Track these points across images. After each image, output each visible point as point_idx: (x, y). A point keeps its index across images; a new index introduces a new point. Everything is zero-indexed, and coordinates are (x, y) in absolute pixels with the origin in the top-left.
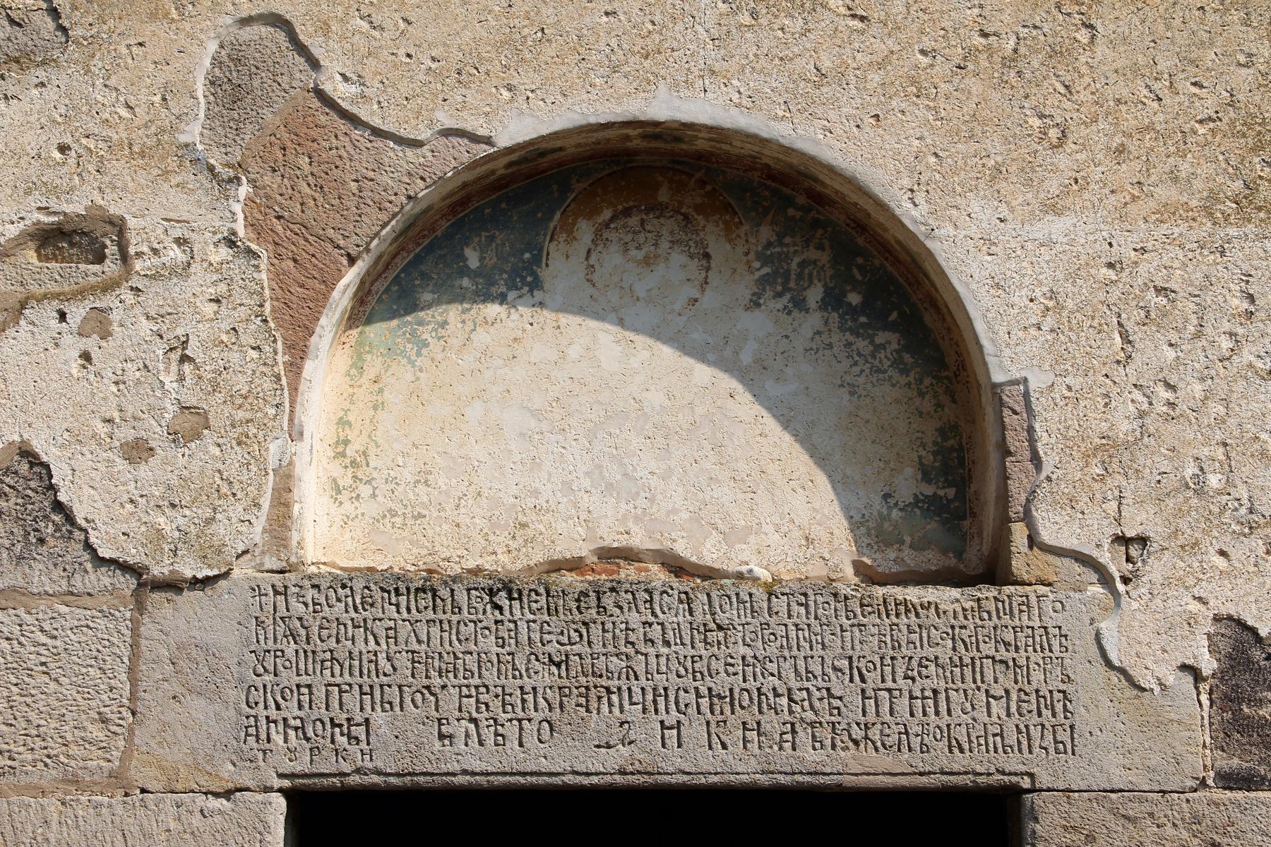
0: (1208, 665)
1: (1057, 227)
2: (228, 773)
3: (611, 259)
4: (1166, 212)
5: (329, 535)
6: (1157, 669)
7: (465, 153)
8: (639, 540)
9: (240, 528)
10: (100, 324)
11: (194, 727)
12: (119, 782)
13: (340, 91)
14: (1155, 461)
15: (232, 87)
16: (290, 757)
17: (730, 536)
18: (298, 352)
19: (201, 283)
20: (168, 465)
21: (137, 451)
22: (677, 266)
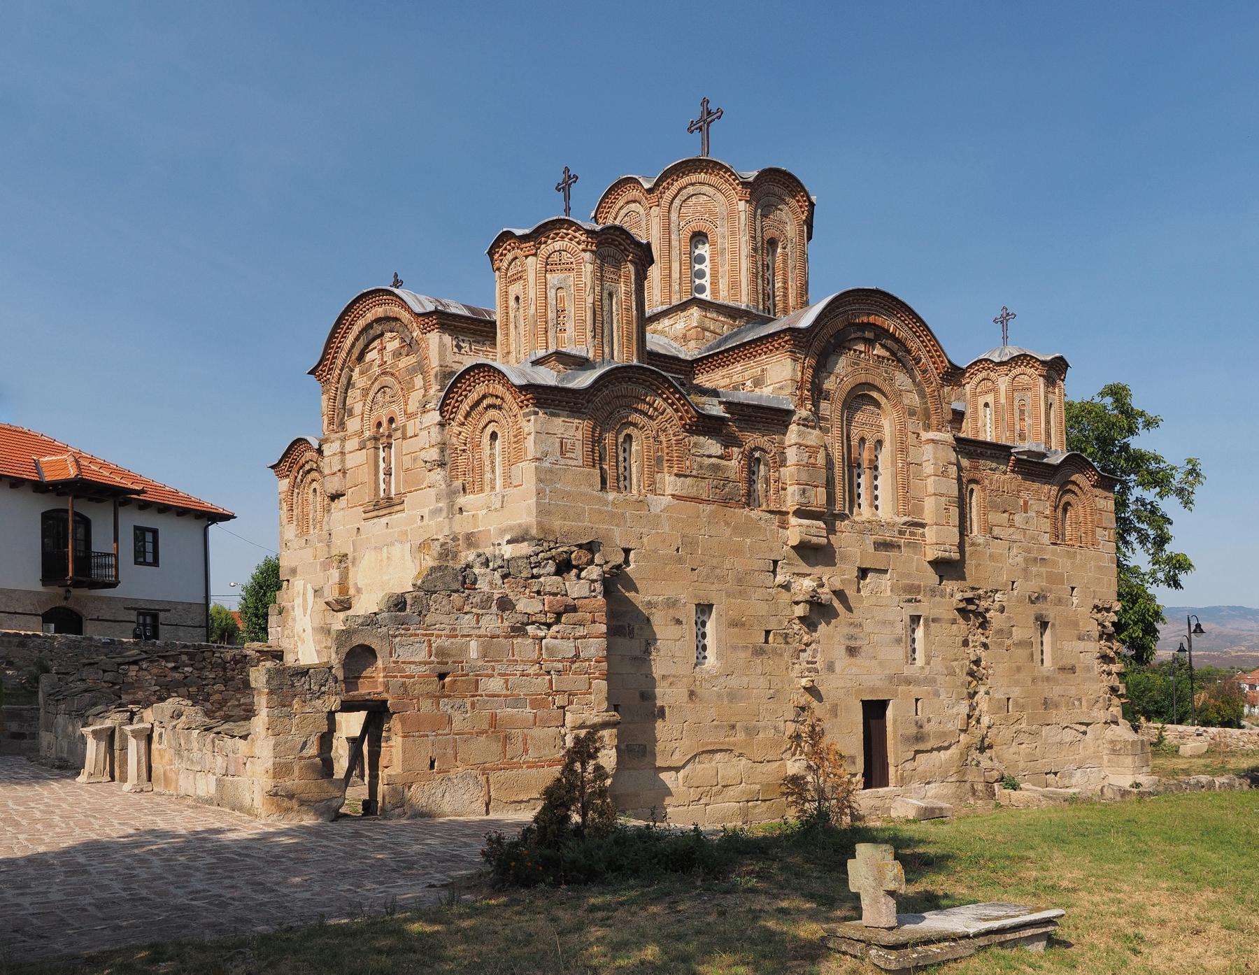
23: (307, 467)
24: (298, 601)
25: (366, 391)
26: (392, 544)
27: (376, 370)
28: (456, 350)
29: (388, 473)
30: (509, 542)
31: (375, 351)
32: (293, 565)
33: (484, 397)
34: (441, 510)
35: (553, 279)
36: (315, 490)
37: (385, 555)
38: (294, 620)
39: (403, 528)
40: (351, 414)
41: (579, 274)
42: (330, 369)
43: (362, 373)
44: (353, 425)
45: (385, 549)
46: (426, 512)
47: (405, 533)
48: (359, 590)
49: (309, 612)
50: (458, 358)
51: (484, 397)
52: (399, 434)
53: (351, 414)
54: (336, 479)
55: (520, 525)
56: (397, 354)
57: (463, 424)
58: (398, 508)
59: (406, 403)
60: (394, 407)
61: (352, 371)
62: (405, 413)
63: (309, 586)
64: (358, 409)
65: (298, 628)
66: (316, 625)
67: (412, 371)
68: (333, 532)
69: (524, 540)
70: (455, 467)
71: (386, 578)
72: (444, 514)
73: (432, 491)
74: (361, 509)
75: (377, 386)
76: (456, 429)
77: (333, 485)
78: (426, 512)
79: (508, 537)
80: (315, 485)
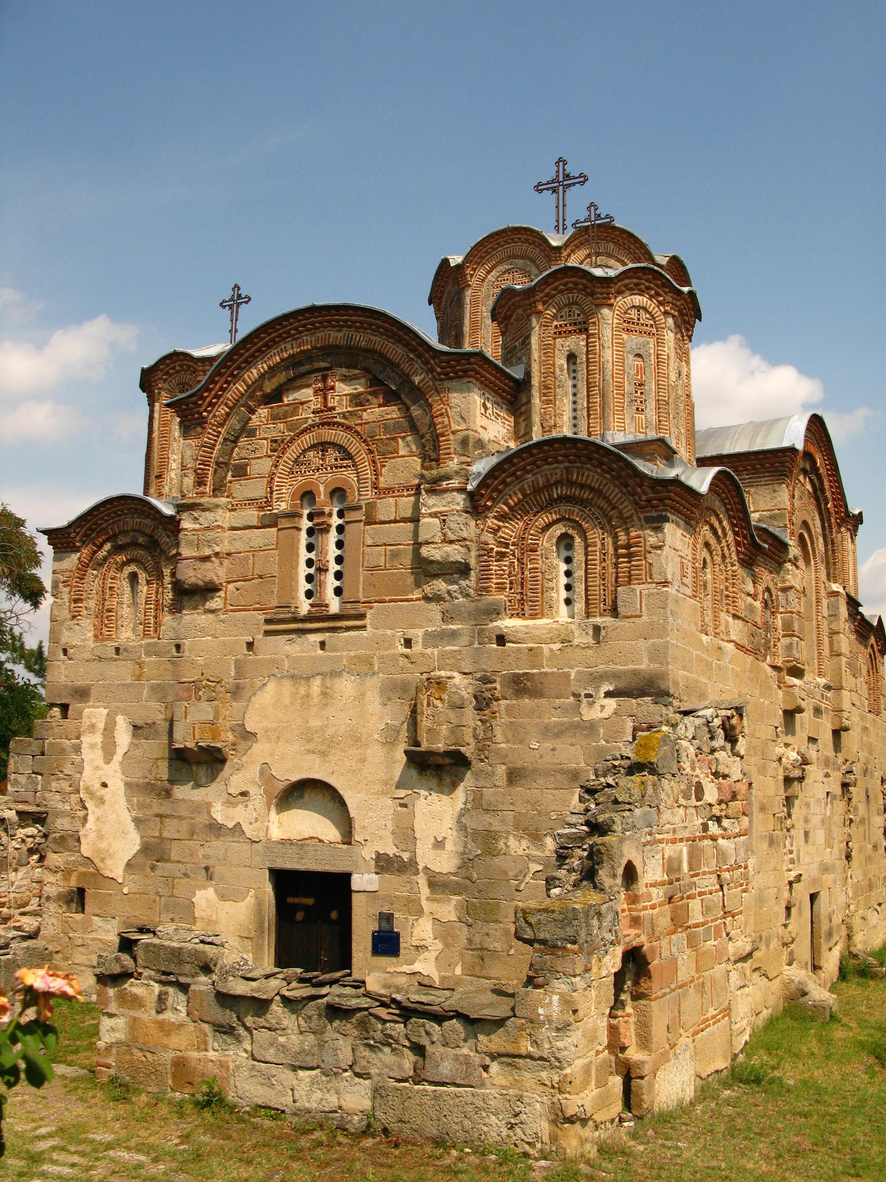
0: (374, 857)
1: (358, 795)
2: (262, 866)
3: (312, 794)
4: (372, 794)
5: (276, 834)
6: (368, 858)
7: (289, 782)
8: (314, 836)
9: (262, 834)
10: (246, 806)
12: (250, 867)
13: (274, 774)
14: (369, 829)
15: (262, 773)
17: (326, 836)
18: (269, 810)
19: (257, 801)
21: (251, 823)
22: (320, 796)
24: (91, 742)
25: (278, 446)
26: (335, 674)
27: (306, 415)
28: (483, 411)
30: (608, 694)
31: (309, 391)
32: (80, 683)
33: (556, 483)
34: (454, 634)
35: (633, 341)
36: (133, 577)
38: (79, 768)
40: (241, 472)
41: (659, 343)
42: (211, 404)
44: (243, 490)
45: (316, 685)
47: (368, 661)
48: (248, 736)
49: (118, 757)
50: (485, 422)
51: (556, 483)
52: (359, 515)
53: (241, 472)
54: (208, 565)
55: (635, 673)
56: (357, 400)
57: (502, 517)
59: (377, 474)
60: (350, 475)
61: (253, 412)
62: (375, 486)
65: (89, 777)
66: (137, 778)
67: (397, 427)
68: (186, 643)
69: (642, 693)
70: (484, 577)
71: (315, 723)
72: (465, 640)
73: (435, 609)
74: (262, 618)
75: (308, 439)
76: (491, 522)
77: (191, 574)
78: (417, 634)
80: (133, 568)
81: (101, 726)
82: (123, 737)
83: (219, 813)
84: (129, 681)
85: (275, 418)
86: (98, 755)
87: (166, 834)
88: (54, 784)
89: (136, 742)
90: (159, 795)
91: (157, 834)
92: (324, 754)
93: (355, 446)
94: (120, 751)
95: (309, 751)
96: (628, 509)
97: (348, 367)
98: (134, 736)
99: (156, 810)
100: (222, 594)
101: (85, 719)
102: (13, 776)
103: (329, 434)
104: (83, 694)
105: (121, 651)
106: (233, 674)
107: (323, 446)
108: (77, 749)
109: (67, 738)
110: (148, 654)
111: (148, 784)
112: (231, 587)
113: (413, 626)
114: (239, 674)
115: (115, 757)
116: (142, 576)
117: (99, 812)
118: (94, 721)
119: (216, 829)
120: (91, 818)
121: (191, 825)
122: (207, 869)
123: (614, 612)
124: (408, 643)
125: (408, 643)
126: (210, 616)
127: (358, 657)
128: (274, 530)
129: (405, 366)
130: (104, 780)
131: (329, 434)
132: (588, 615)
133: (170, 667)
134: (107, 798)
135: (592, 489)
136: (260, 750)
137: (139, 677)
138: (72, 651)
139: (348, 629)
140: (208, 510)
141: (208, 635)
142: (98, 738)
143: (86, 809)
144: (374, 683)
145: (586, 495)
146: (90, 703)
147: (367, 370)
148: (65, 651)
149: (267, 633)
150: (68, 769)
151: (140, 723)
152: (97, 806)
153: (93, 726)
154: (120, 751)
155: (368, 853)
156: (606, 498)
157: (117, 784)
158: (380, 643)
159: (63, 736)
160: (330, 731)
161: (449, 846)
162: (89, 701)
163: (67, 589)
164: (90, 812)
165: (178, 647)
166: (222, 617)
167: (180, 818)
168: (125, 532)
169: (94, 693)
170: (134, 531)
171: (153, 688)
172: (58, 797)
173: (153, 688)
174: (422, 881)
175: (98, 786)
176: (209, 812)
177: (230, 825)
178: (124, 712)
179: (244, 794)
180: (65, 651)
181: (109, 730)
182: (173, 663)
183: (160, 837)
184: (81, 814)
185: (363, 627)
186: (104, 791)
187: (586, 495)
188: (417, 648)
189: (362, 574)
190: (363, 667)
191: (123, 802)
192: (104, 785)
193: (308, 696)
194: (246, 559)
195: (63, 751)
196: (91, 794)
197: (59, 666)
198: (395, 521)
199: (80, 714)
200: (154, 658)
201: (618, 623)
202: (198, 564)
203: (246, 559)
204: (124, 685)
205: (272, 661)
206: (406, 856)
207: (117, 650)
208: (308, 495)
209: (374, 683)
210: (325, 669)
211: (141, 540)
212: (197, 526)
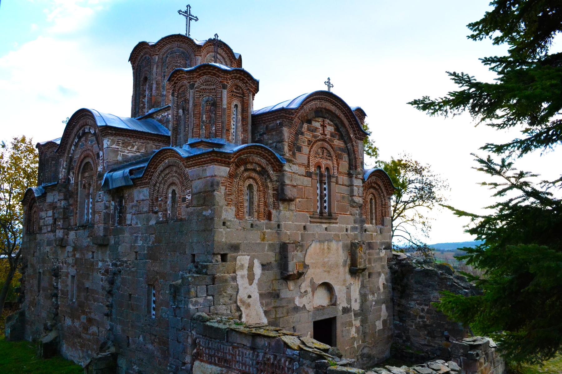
11: (311, 318)
16: (314, 320)
20: (310, 304)
23: (249, 166)
24: (242, 273)
26: (330, 241)
29: (322, 198)
30: (384, 249)
32: (234, 241)
34: (356, 228)
36: (250, 187)
37: (326, 247)
39: (337, 233)
43: (309, 130)
46: (349, 226)
49: (256, 281)
58: (334, 221)
63: (257, 263)
64: (306, 149)
65: (242, 294)
68: (283, 223)
71: (326, 260)
72: (359, 230)
73: (352, 218)
78: (349, 226)
79: (384, 247)
80: (251, 181)
81: (247, 265)
82: (258, 270)
83: (298, 302)
84: (258, 241)
85: (309, 130)
86: (247, 280)
87: (278, 316)
88: (221, 300)
89: (263, 272)
90: (274, 297)
91: (274, 317)
92: (329, 272)
93: (332, 153)
94: (257, 277)
95: (325, 271)
96: (385, 193)
97: (330, 120)
98: (263, 269)
99: (273, 305)
100: (294, 202)
101: (238, 262)
102: (194, 300)
103: (326, 145)
104: (236, 248)
105: (254, 226)
106: (300, 239)
107: (323, 148)
108: (234, 279)
109: (228, 273)
110: (266, 229)
111: (269, 293)
112: (297, 200)
113: (348, 224)
114: (302, 240)
115: (254, 281)
116: (255, 188)
117: (247, 311)
118: (243, 263)
119: (296, 309)
120: (244, 316)
121: (288, 310)
122: (294, 327)
123: (383, 225)
124: (347, 230)
125: (347, 230)
126: (291, 213)
127: (336, 234)
128: (310, 179)
129: (349, 130)
130: (250, 293)
131: (326, 145)
132: (376, 224)
133: (276, 235)
134: (251, 303)
135: (379, 185)
136: (310, 274)
137: (263, 239)
138: (228, 223)
139: (333, 223)
140: (295, 164)
141: (291, 220)
142: (245, 272)
143: (241, 311)
144: (341, 243)
145: (377, 187)
146: (240, 253)
147: (336, 125)
148: (224, 224)
149: (311, 222)
150: (230, 291)
151: (265, 263)
152: (246, 308)
153: (242, 266)
154: (257, 277)
155: (340, 308)
156: (381, 190)
157: (256, 295)
158: (341, 229)
159: (226, 272)
160: (330, 263)
161: (358, 301)
162: (238, 252)
163: (223, 188)
164: (243, 312)
165: (279, 226)
166: (295, 213)
167: (283, 307)
168: (252, 163)
169: (242, 247)
170: (257, 164)
171: (270, 245)
172: (224, 307)
173: (270, 245)
174: (352, 314)
175: (246, 298)
176: (294, 302)
177: (301, 306)
178: (258, 258)
179: (306, 292)
180: (224, 224)
181: (251, 267)
182: (278, 234)
183: (276, 318)
184: (237, 314)
185: (336, 223)
186: (249, 300)
187: (377, 187)
188: (349, 232)
189: (336, 203)
190: (337, 238)
191: (259, 304)
192: (250, 297)
193: (324, 249)
194: (302, 189)
195: (226, 281)
196: (243, 302)
197: (221, 232)
198: (343, 185)
199: (235, 259)
200: (269, 230)
201: (385, 228)
202: (292, 188)
203: (302, 189)
204: (256, 243)
205: (313, 234)
206: (349, 306)
207: (252, 225)
208: (319, 167)
209: (341, 243)
210: (328, 238)
211: (258, 169)
212: (290, 171)
